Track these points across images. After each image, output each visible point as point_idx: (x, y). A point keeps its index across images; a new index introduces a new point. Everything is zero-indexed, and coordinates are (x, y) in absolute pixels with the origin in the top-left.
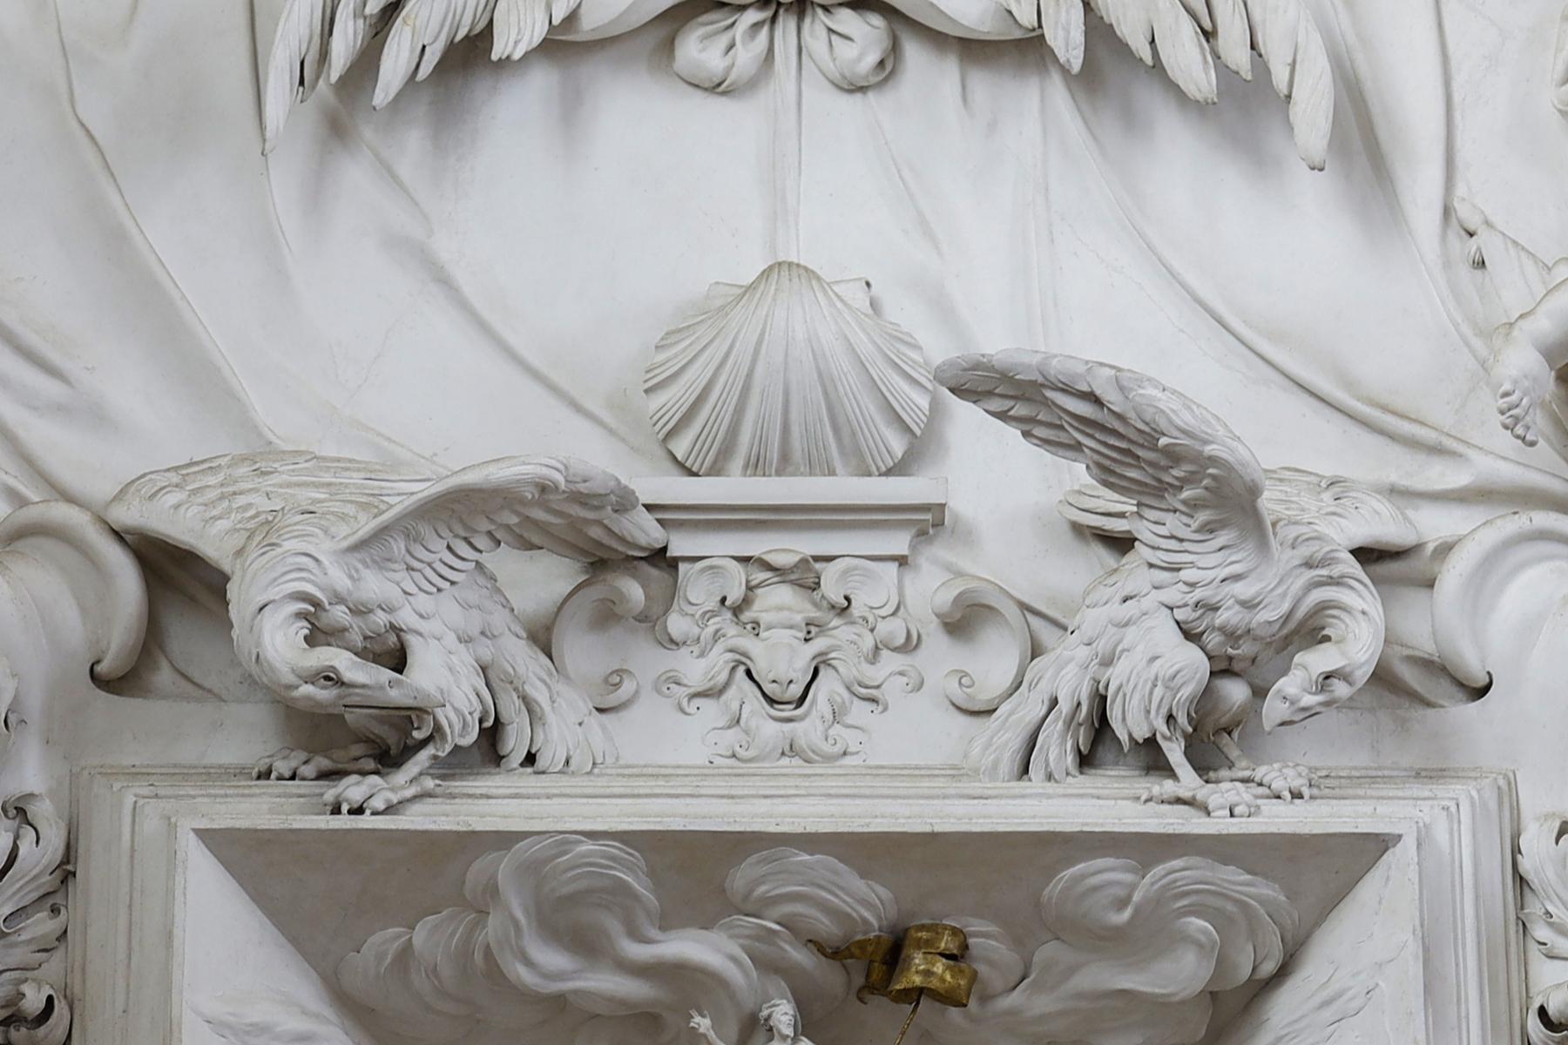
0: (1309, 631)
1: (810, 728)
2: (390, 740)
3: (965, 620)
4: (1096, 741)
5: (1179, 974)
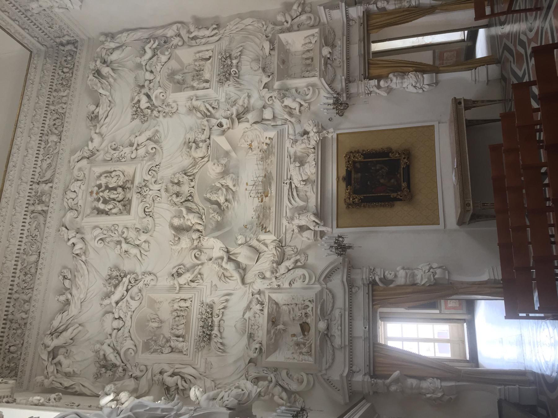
0: (257, 299)
1: (260, 326)
2: (261, 349)
3: (255, 317)
4: (262, 310)
5: (275, 306)
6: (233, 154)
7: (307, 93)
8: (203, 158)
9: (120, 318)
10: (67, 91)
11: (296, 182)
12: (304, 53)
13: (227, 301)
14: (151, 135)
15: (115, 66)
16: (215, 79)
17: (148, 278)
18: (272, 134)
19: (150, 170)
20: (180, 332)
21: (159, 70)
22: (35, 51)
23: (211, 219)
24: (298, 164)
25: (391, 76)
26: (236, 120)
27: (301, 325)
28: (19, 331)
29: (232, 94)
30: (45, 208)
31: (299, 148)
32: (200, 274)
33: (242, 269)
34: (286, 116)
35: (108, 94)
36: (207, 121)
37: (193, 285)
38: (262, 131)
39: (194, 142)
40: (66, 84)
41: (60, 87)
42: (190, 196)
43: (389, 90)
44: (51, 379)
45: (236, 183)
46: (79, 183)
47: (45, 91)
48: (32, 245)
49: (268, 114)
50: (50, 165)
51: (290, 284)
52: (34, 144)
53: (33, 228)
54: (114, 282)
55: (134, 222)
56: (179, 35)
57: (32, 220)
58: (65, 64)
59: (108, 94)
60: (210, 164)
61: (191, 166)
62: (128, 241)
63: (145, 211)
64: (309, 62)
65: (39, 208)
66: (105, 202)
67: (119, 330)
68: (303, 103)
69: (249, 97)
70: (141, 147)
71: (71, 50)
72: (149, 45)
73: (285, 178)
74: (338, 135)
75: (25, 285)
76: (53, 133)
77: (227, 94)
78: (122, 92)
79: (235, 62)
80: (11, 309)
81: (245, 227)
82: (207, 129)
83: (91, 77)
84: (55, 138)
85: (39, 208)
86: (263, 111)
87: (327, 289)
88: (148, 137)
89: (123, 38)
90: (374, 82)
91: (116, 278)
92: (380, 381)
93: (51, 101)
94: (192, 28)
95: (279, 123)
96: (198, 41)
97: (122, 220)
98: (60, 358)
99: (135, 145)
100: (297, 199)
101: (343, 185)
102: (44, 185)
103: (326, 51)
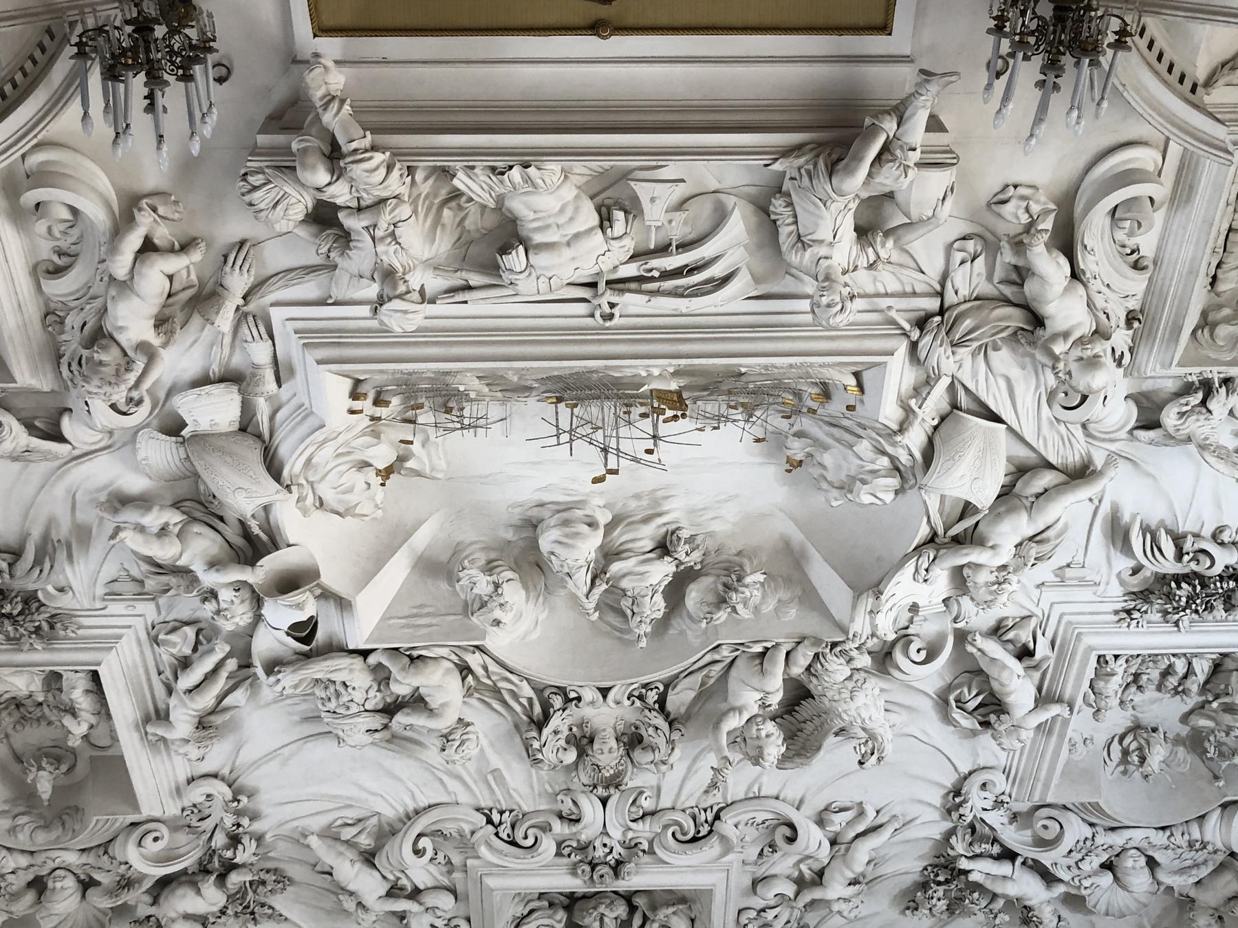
6: (422, 539)
7: (66, 214)
8: (465, 670)
9: (1108, 866)
11: (607, 254)
13: (1148, 531)
14: (351, 854)
16: (40, 655)
17: (977, 802)
18: (330, 391)
19: (513, 843)
21: (23, 861)
23: (757, 609)
24: (516, 259)
26: (271, 564)
29: (110, 570)
31: (418, 245)
32: (997, 631)
33: (1022, 481)
34: (225, 319)
36: (273, 667)
37: (1042, 649)
38: (319, 436)
39: (390, 710)
42: (641, 698)
45: (566, 513)
49: (214, 411)
51: (1136, 266)
55: (736, 866)
60: (497, 642)
61: (496, 705)
62: (808, 874)
63: (695, 840)
67: (1152, 863)
68: (134, 241)
69: (121, 501)
70: (404, 882)
73: (581, 308)
74: (321, 30)
77: (113, 595)
81: (794, 465)
82: (319, 669)
86: (198, 437)
87: (1209, 82)
88: (358, 865)
95: (260, 353)
99: (402, 905)
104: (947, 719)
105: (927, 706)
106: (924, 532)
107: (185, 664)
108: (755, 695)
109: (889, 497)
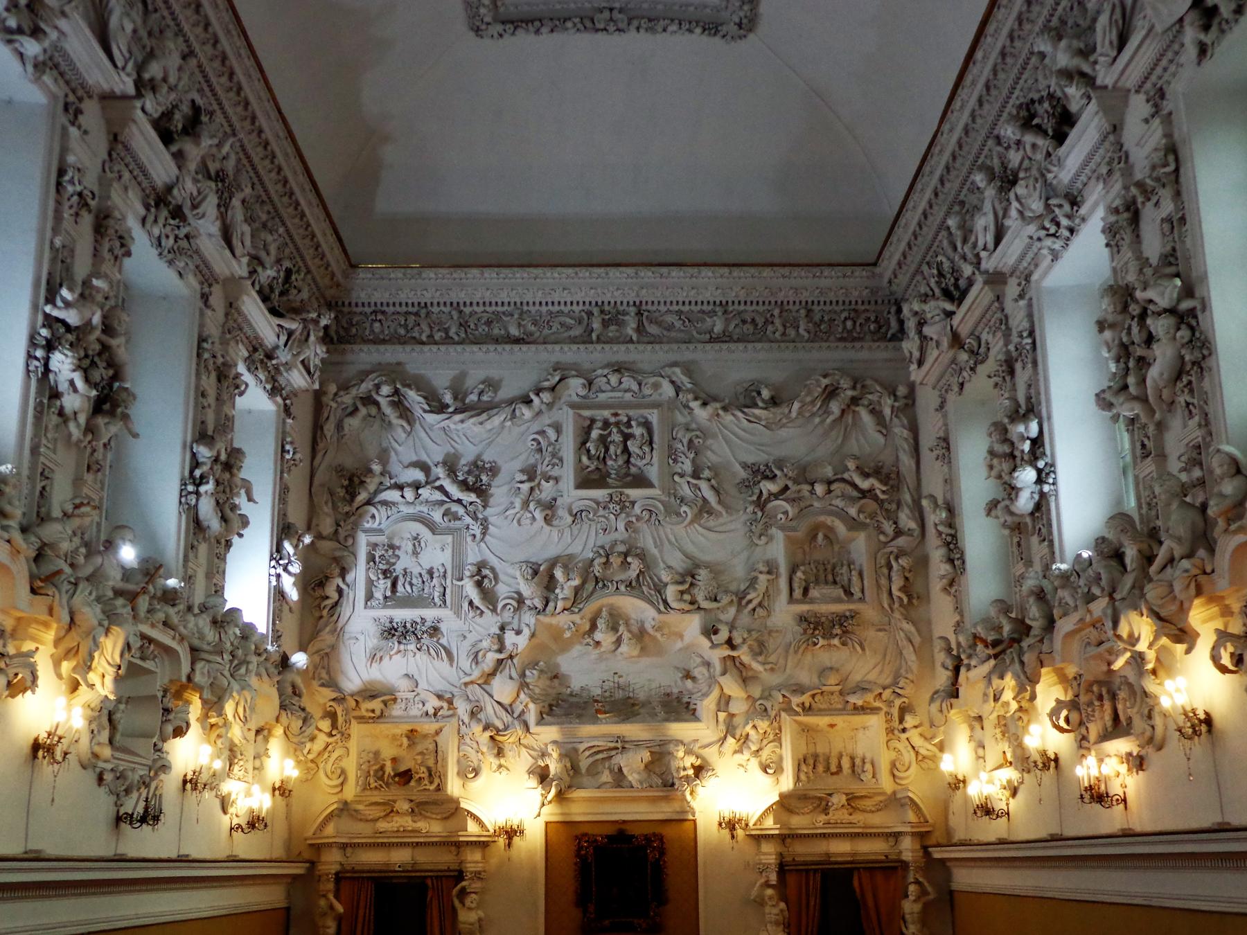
10: (806, 335)
12: (852, 759)
15: (849, 418)
17: (476, 529)
20: (400, 588)
21: (833, 502)
22: (877, 270)
25: (782, 905)
27: (410, 770)
28: (402, 331)
30: (594, 336)
35: (794, 414)
37: (465, 605)
39: (692, 584)
40: (822, 330)
41: (817, 318)
43: (760, 903)
44: (334, 405)
46: (635, 387)
47: (805, 296)
48: (535, 323)
50: (670, 327)
52: (708, 295)
53: (562, 319)
54: (471, 480)
56: (898, 533)
57: (577, 314)
58: (861, 320)
59: (794, 414)
64: (833, 768)
65: (596, 325)
66: (603, 440)
71: (889, 327)
72: (877, 485)
75: (472, 326)
76: (727, 321)
78: (796, 437)
79: (836, 641)
80: (435, 309)
83: (825, 382)
84: (718, 328)
85: (596, 325)
89: (900, 431)
90: (773, 878)
91: (477, 479)
92: (331, 886)
93: (791, 307)
94: (903, 562)
96: (885, 571)
97: (568, 474)
98: (363, 411)
100: (591, 760)
101: (610, 831)
102: (634, 325)
103: (838, 800)
104: (493, 570)
105: (501, 576)
106: (515, 661)
107: (760, 605)
108: (566, 586)
109: (528, 673)
